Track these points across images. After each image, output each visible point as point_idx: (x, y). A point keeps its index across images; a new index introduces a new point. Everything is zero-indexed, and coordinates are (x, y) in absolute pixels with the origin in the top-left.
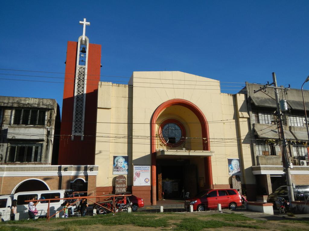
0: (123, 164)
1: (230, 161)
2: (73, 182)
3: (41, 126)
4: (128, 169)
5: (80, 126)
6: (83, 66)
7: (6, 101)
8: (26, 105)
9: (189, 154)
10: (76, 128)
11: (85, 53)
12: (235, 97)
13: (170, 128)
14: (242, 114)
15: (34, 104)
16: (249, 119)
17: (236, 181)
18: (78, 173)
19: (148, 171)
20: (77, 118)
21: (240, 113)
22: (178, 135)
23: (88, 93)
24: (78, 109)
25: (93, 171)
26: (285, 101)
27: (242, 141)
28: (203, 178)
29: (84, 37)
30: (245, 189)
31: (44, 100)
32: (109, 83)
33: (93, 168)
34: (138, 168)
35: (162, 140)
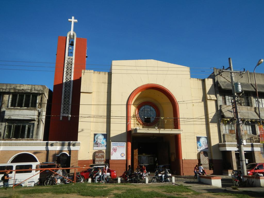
0: (102, 140)
1: (198, 139)
2: (59, 155)
3: (33, 108)
4: (106, 145)
5: (68, 108)
6: (71, 57)
7: (4, 88)
8: (21, 91)
9: (159, 132)
10: (64, 110)
11: (73, 46)
12: (203, 81)
13: (146, 109)
14: (210, 96)
15: (27, 90)
16: (216, 101)
17: (204, 156)
18: (62, 148)
20: (65, 101)
21: (208, 96)
22: (153, 115)
23: (75, 80)
24: (66, 93)
25: (75, 146)
26: (239, 83)
27: (210, 120)
28: (174, 153)
29: (72, 32)
30: (212, 164)
31: (36, 86)
32: (91, 71)
33: (75, 144)
34: (115, 144)
35: (138, 120)
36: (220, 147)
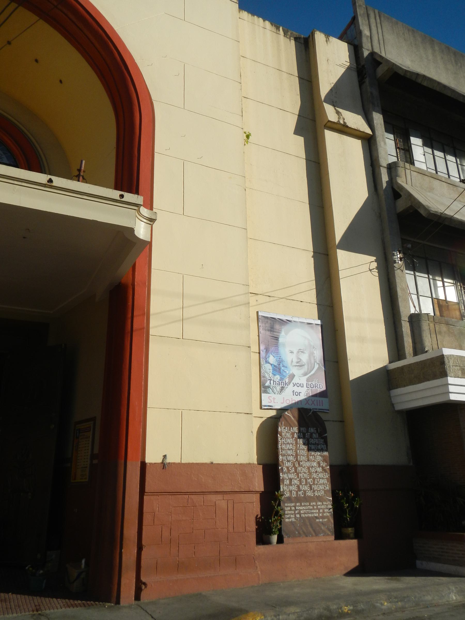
28: (93, 419)
36: (397, 387)
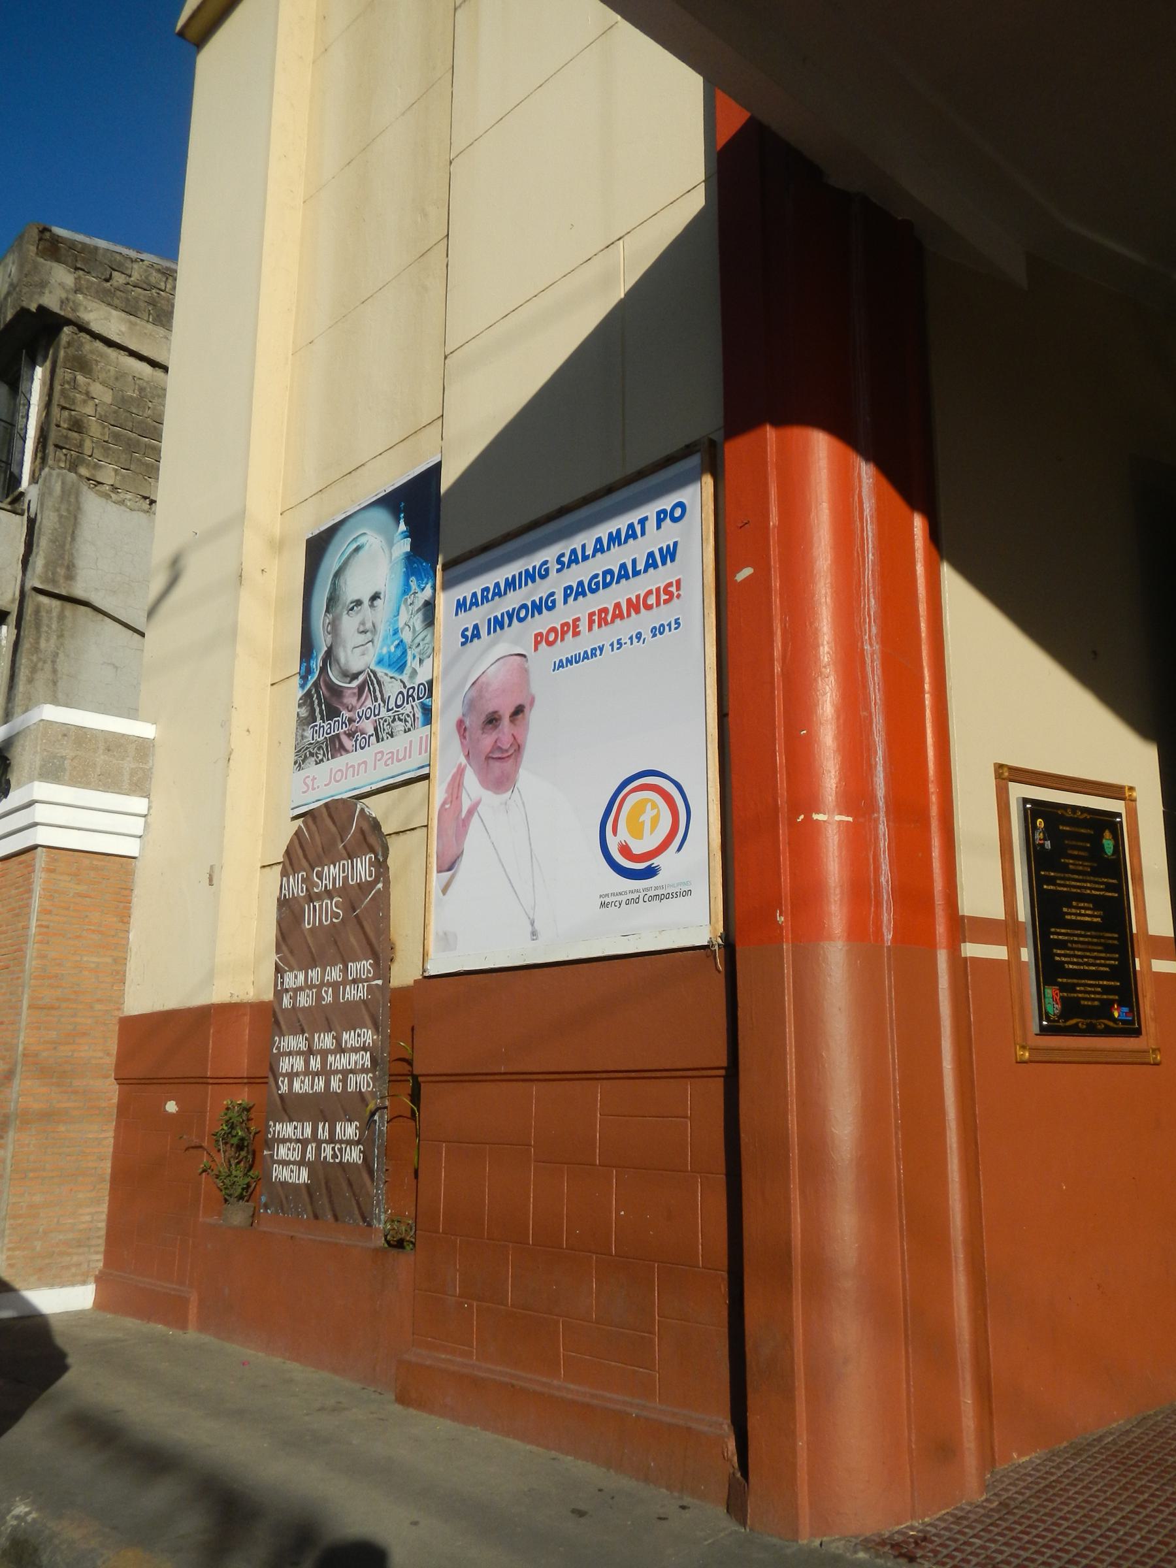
19: (669, 593)
